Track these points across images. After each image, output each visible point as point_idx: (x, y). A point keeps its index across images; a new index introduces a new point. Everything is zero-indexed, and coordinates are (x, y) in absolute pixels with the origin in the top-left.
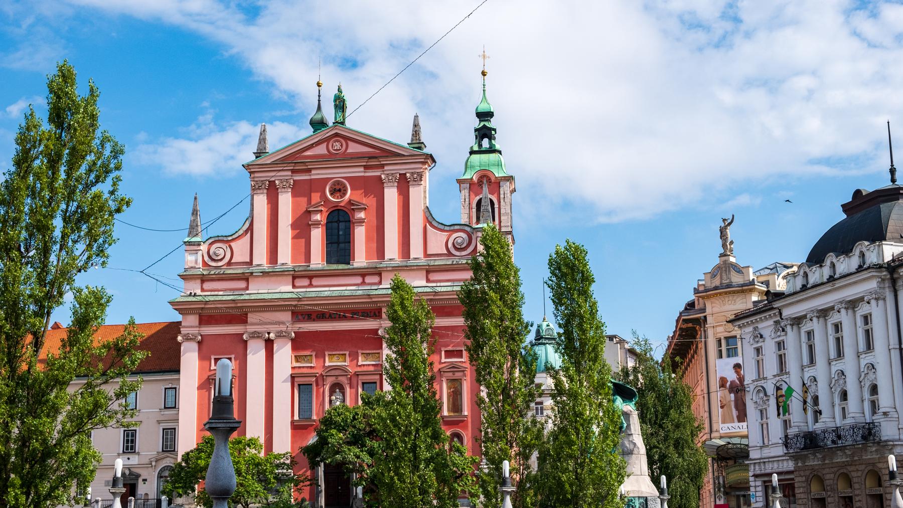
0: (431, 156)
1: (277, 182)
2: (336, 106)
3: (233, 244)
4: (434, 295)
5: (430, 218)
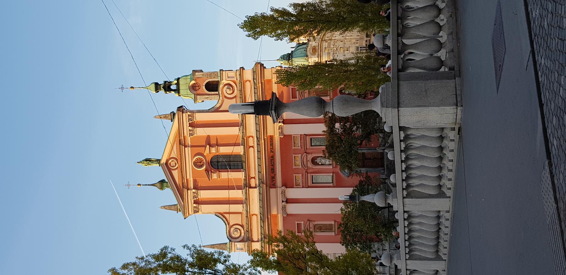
0: (179, 108)
3: (231, 224)
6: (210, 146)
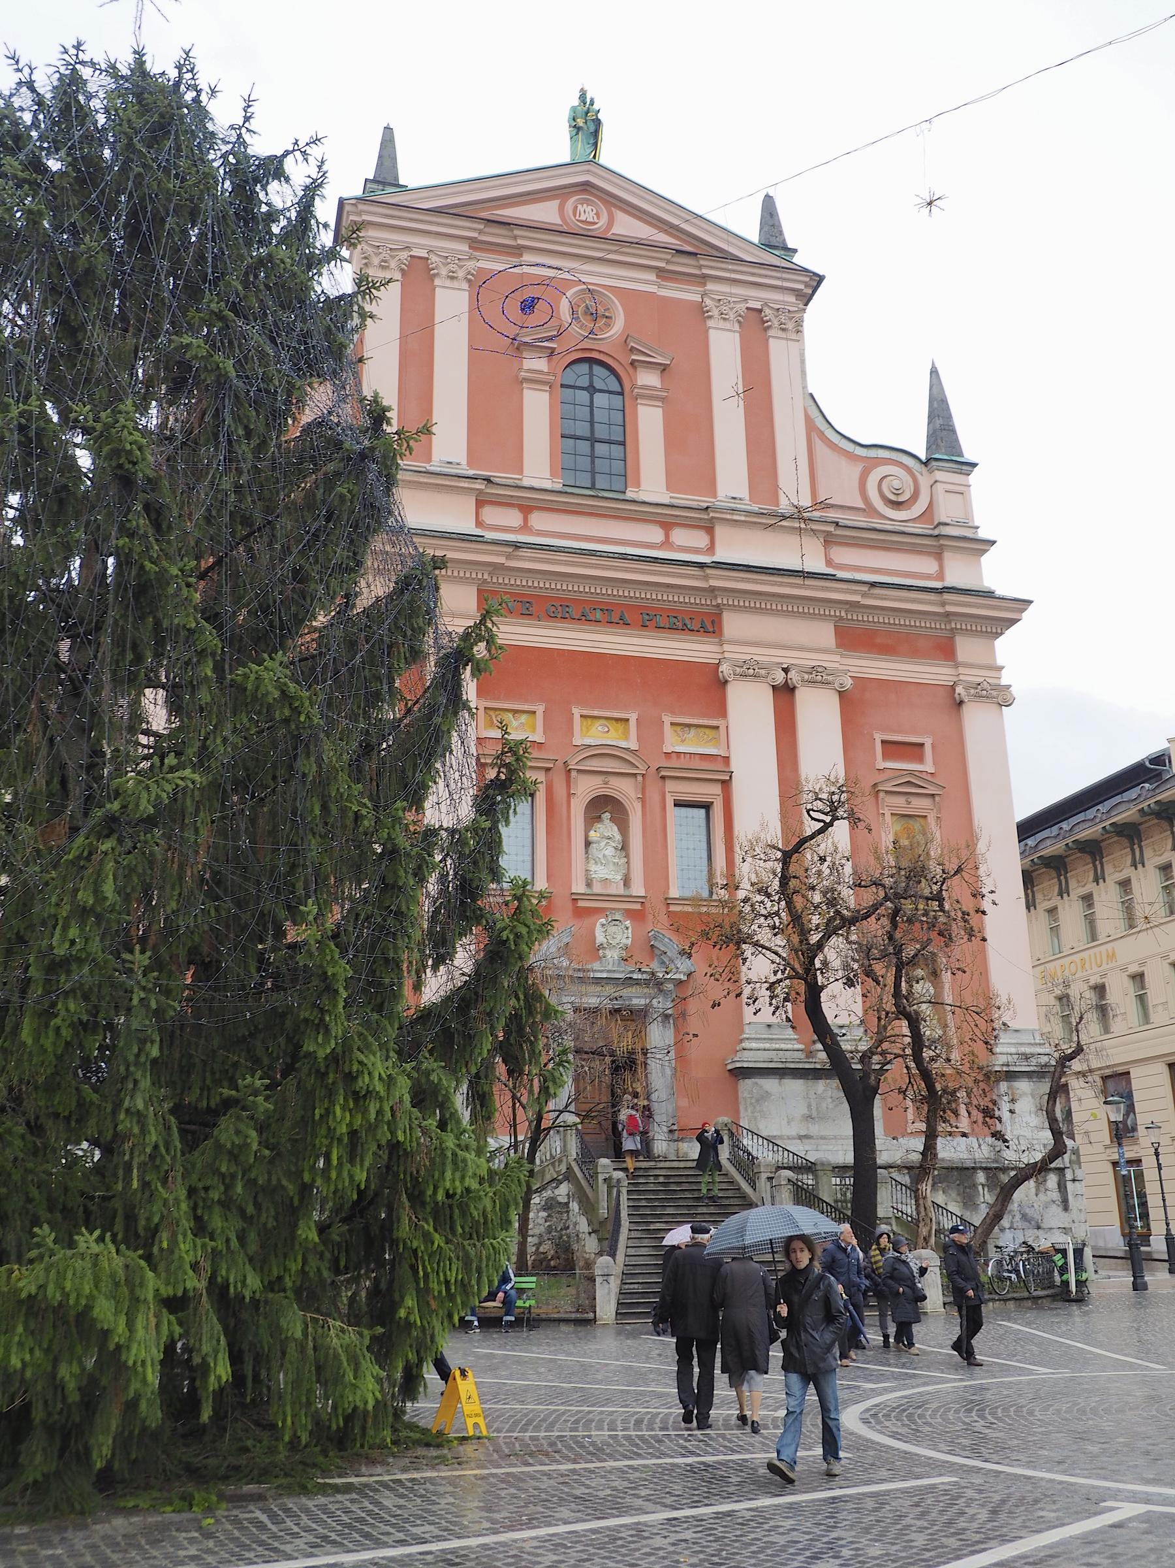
0: (820, 279)
1: (434, 258)
2: (577, 129)
4: (864, 595)
5: (820, 422)
6: (664, 369)
